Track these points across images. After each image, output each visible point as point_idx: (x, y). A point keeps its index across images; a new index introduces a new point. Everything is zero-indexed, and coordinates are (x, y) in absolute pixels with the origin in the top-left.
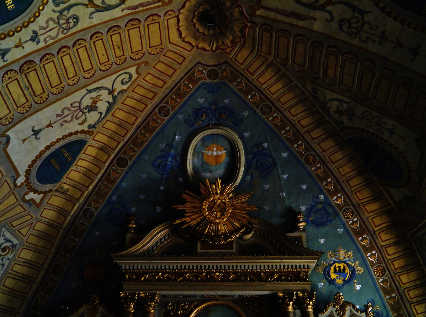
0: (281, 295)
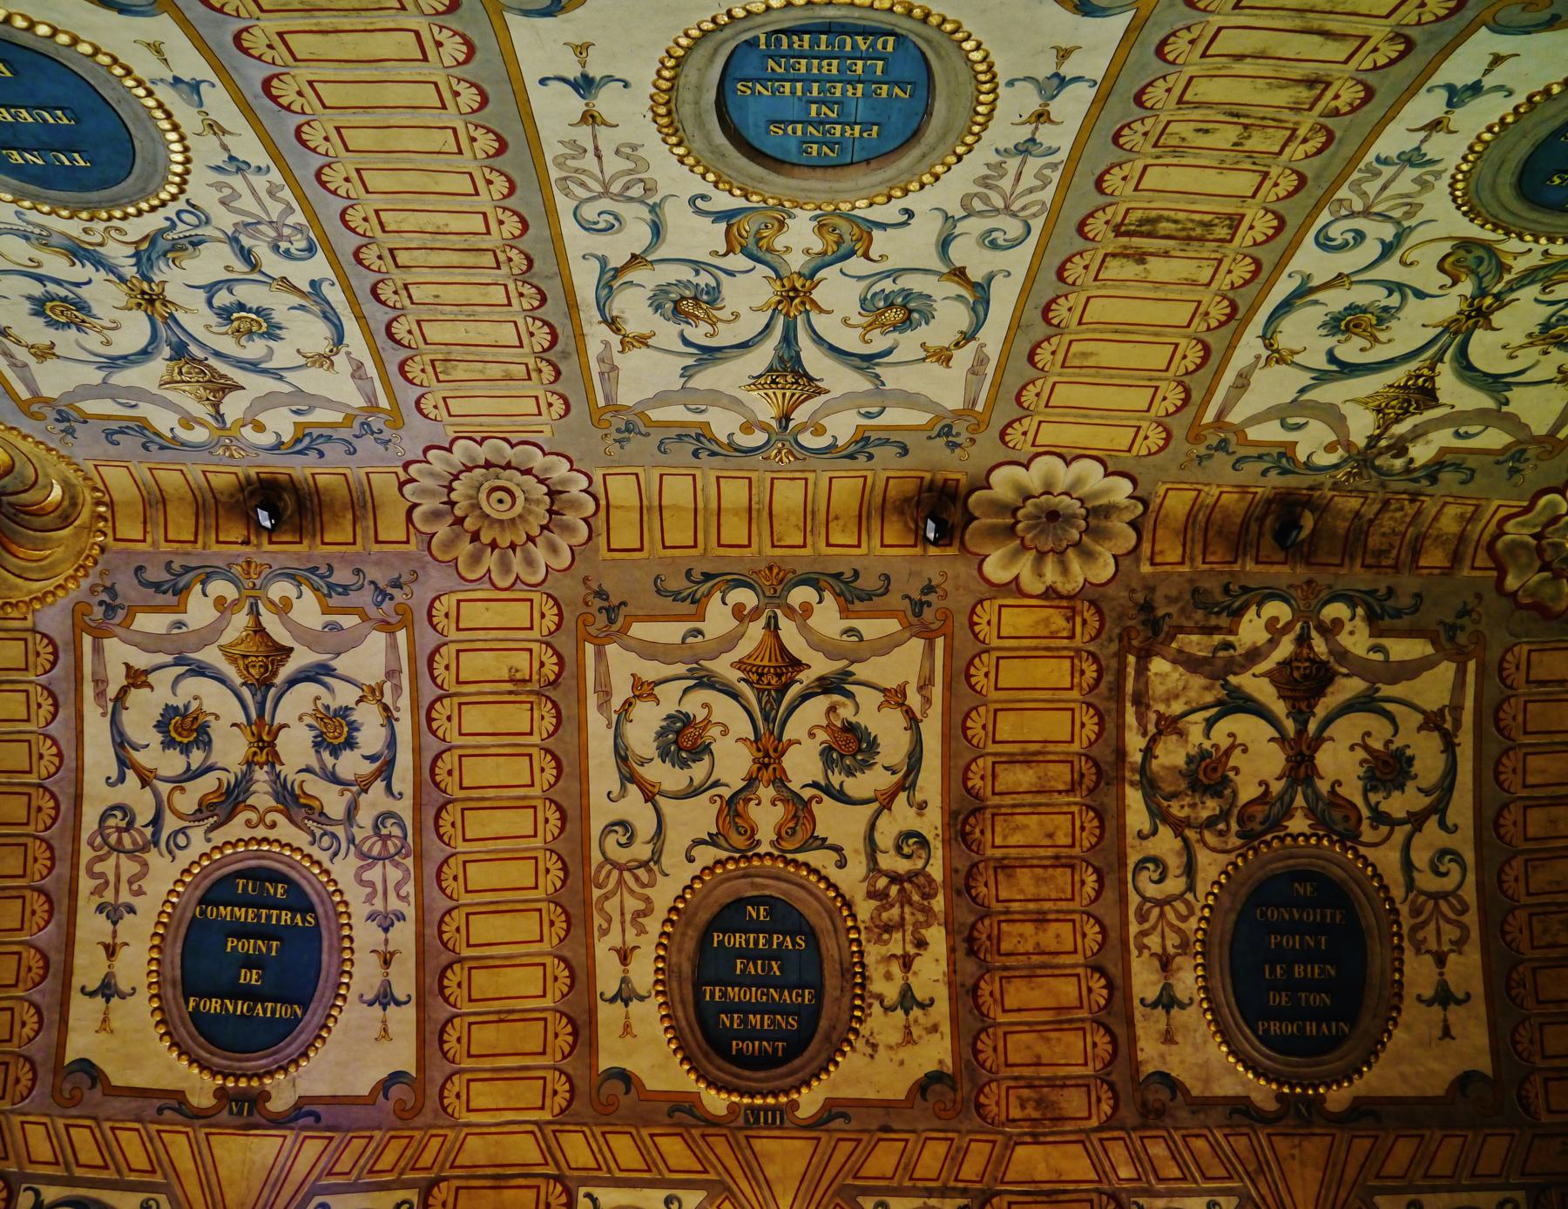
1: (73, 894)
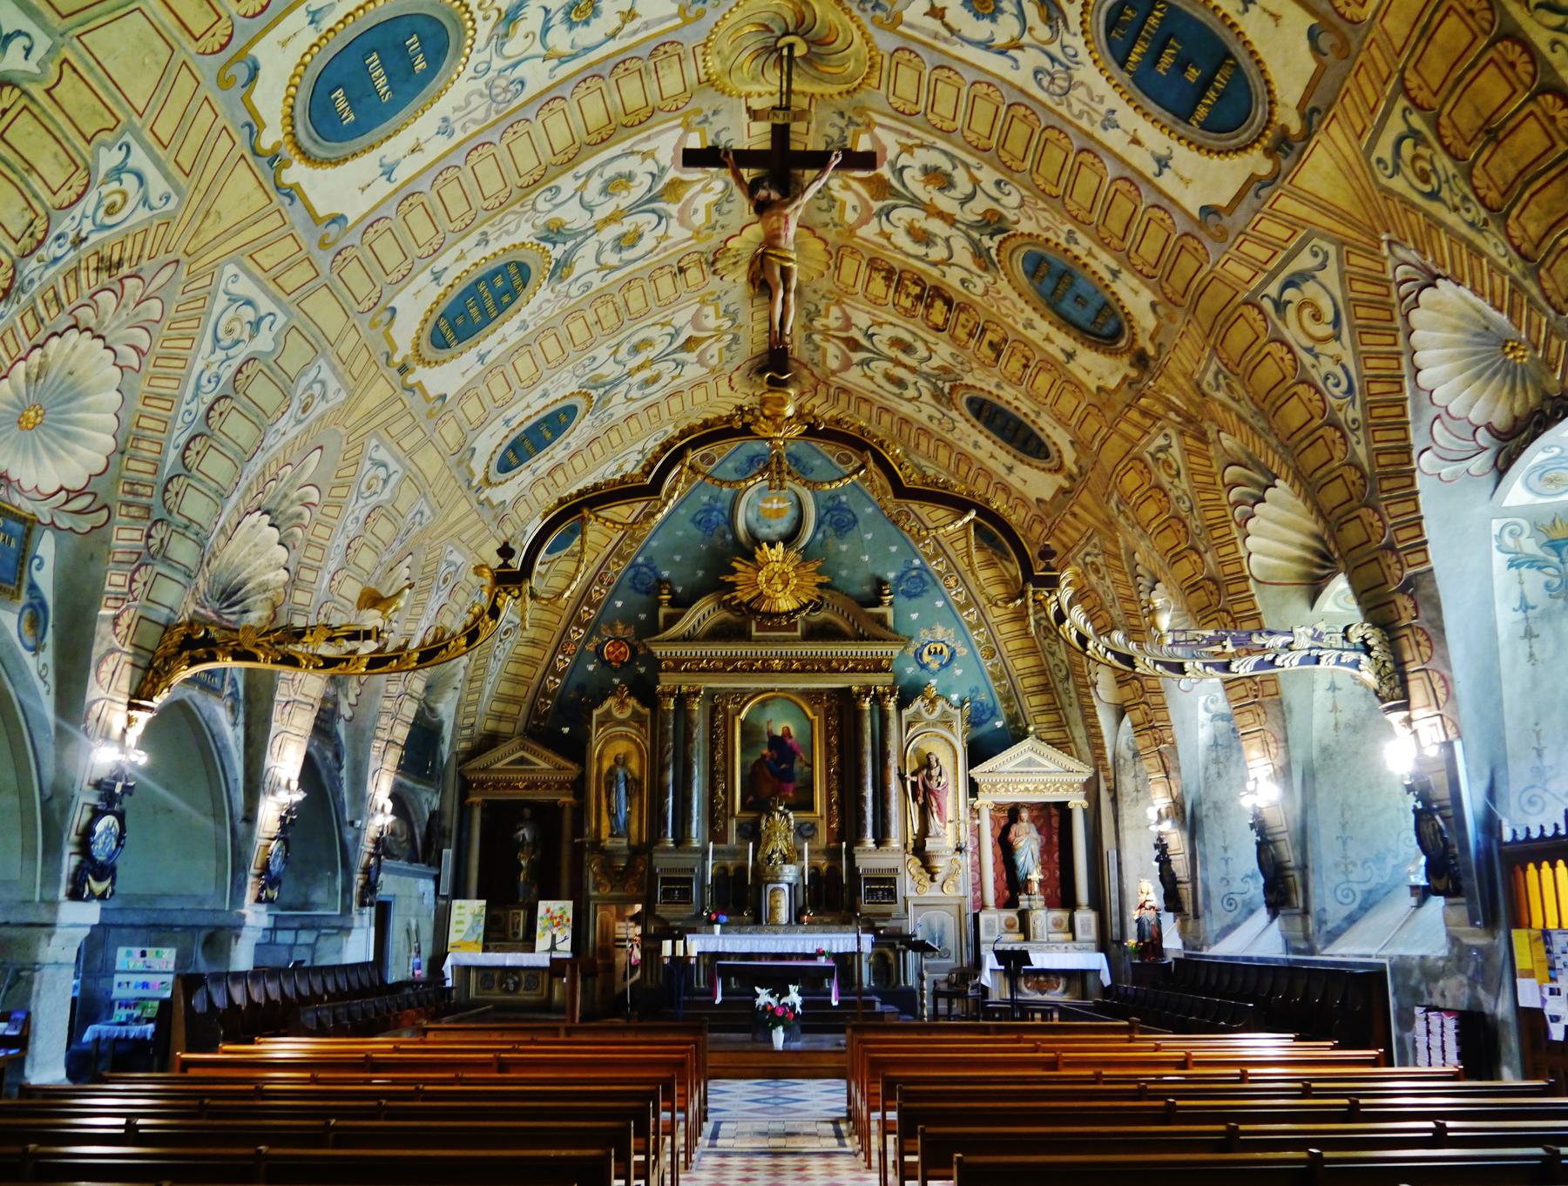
0: (855, 689)
1: (1090, 136)
